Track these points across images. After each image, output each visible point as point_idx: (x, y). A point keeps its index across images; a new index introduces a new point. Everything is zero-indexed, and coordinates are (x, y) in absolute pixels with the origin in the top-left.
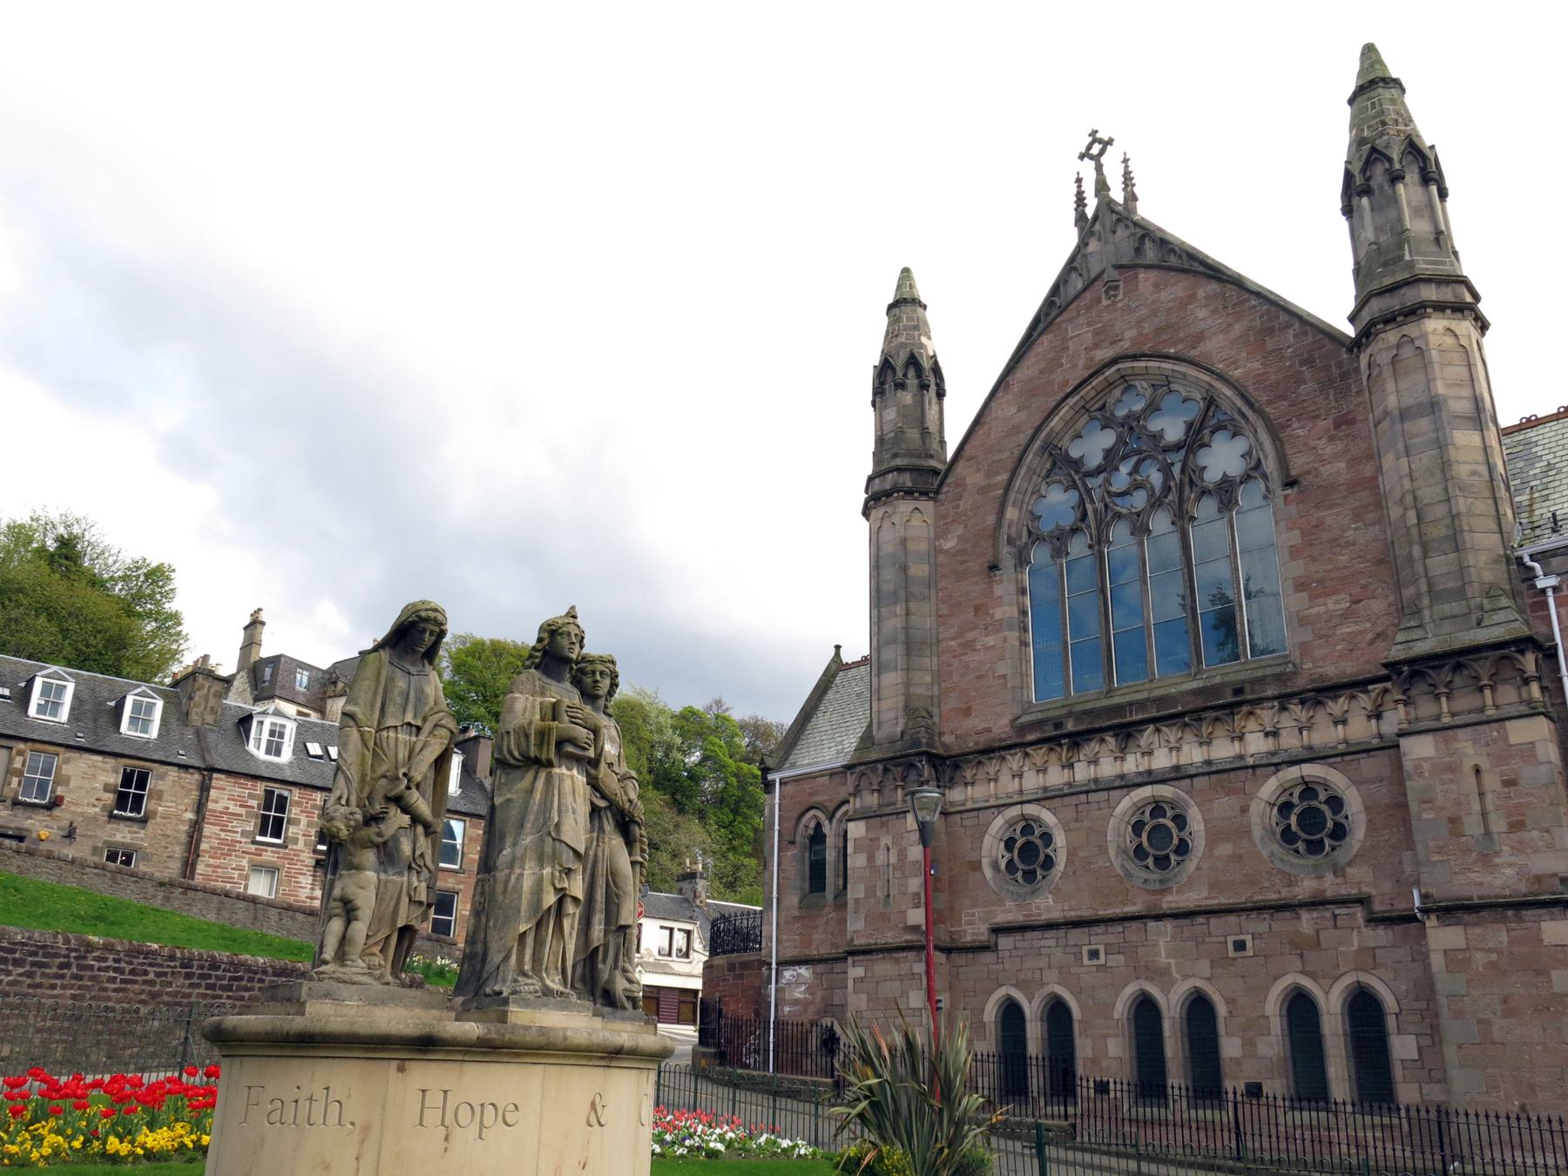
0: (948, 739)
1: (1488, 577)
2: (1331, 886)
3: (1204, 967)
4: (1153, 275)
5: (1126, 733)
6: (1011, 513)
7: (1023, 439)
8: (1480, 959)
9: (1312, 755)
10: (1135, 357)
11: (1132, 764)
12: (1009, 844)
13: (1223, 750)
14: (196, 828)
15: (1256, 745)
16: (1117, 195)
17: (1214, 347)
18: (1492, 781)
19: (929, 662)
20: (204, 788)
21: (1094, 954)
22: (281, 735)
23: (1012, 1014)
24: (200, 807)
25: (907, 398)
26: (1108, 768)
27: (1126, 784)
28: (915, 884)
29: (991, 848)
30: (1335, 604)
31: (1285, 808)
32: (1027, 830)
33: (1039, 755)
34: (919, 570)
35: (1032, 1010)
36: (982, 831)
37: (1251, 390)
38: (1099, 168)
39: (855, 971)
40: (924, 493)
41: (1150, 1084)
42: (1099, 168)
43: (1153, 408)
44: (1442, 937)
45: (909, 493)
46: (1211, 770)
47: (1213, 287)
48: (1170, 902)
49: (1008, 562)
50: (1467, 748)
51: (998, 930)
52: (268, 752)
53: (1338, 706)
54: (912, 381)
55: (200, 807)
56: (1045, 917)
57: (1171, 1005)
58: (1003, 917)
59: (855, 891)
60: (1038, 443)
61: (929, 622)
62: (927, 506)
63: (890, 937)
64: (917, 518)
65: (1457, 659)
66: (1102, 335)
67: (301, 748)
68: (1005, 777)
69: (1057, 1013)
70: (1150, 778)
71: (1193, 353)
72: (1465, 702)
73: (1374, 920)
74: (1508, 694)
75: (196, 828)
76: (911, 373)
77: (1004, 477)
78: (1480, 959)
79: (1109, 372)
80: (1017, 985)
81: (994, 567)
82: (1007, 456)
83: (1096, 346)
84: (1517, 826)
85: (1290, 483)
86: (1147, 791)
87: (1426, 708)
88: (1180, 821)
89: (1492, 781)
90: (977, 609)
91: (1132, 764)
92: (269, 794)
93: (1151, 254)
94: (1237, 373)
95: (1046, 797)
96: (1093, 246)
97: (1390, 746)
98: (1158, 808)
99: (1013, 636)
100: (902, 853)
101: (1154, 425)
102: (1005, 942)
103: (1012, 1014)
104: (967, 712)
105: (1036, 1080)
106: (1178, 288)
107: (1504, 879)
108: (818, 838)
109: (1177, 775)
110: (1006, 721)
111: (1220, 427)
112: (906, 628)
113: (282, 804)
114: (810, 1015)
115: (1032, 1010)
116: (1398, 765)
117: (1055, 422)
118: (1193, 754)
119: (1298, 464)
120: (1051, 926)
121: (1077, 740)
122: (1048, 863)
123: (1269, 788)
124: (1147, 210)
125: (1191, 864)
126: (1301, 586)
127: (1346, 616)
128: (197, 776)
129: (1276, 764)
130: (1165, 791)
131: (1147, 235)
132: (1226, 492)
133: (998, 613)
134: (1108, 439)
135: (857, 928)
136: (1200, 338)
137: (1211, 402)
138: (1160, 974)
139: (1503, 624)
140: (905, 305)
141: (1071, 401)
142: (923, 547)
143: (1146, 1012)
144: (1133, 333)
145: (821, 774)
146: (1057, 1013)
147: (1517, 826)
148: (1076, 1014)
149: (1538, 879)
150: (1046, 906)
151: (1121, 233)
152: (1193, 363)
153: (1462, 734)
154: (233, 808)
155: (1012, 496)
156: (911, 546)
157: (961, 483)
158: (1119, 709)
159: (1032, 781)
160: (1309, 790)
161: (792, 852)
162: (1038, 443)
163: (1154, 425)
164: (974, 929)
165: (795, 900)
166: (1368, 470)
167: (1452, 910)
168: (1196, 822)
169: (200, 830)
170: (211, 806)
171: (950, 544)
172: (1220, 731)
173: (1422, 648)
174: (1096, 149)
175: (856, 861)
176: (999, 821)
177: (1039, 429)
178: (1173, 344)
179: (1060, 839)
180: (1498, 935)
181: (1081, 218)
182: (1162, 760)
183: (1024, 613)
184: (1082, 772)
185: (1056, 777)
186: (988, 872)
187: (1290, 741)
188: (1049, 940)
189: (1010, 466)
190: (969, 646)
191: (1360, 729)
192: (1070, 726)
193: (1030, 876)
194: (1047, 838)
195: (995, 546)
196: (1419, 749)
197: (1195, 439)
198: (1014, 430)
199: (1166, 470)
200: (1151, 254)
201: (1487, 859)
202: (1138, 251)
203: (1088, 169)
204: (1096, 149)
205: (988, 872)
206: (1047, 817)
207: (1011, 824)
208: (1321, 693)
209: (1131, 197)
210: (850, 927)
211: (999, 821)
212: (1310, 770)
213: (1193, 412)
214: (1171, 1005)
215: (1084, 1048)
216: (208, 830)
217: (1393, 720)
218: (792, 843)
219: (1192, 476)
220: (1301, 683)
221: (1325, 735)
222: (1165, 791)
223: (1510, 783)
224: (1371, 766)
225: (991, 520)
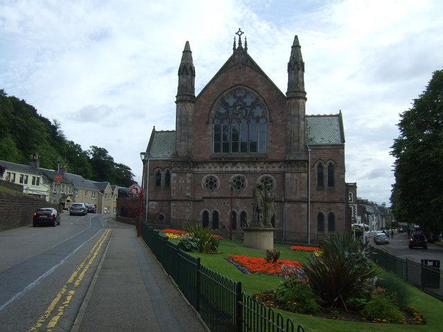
0: (194, 158)
3: (245, 207)
4: (249, 69)
5: (235, 163)
6: (213, 112)
11: (234, 169)
12: (207, 181)
13: (252, 169)
15: (259, 169)
16: (244, 47)
17: (260, 89)
18: (298, 182)
21: (224, 204)
23: (206, 214)
26: (229, 169)
27: (233, 173)
28: (188, 188)
29: (203, 181)
30: (276, 146)
32: (211, 179)
33: (216, 164)
35: (210, 213)
36: (201, 178)
37: (266, 101)
38: (240, 38)
39: (173, 204)
41: (233, 226)
42: (240, 38)
43: (245, 97)
44: (287, 205)
46: (250, 172)
47: (259, 76)
48: (240, 195)
50: (295, 176)
51: (204, 198)
53: (274, 165)
56: (214, 196)
57: (238, 213)
58: (205, 195)
59: (173, 188)
62: (193, 105)
63: (182, 198)
64: (190, 107)
65: (296, 162)
68: (207, 167)
69: (216, 214)
70: (238, 172)
72: (296, 168)
73: (275, 202)
74: (303, 168)
77: (212, 103)
80: (208, 208)
83: (236, 80)
85: (271, 122)
86: (237, 175)
87: (290, 168)
88: (243, 181)
89: (298, 182)
90: (203, 131)
91: (234, 169)
93: (249, 63)
95: (217, 173)
96: (236, 56)
97: (283, 173)
98: (239, 178)
100: (185, 181)
101: (245, 100)
102: (206, 200)
103: (206, 214)
104: (200, 153)
105: (210, 225)
106: (253, 74)
107: (298, 197)
108: (159, 174)
109: (243, 172)
110: (208, 156)
111: (258, 105)
114: (156, 212)
115: (210, 213)
116: (284, 176)
118: (246, 169)
119: (273, 118)
120: (217, 198)
121: (224, 163)
122: (215, 186)
124: (249, 52)
125: (245, 189)
126: (271, 142)
130: (241, 175)
131: (249, 59)
132: (258, 119)
133: (208, 133)
134: (235, 100)
135: (174, 195)
136: (257, 86)
137: (257, 99)
138: (238, 208)
139: (303, 157)
140: (187, 52)
143: (234, 213)
145: (160, 160)
146: (216, 214)
147: (301, 189)
148: (220, 214)
149: (303, 198)
150: (215, 194)
151: (243, 56)
152: (255, 91)
155: (213, 108)
158: (233, 158)
159: (213, 169)
161: (152, 176)
163: (245, 100)
164: (199, 197)
165: (153, 187)
166: (285, 123)
167: (289, 202)
168: (246, 182)
171: (198, 115)
173: (291, 158)
174: (240, 33)
175: (173, 182)
176: (206, 177)
179: (219, 181)
180: (295, 206)
181: (234, 48)
182: (240, 169)
184: (224, 169)
185: (218, 169)
186: (203, 187)
187: (265, 169)
188: (215, 200)
191: (277, 169)
192: (223, 160)
193: (211, 188)
194: (215, 181)
195: (208, 119)
196: (288, 175)
197: (253, 106)
199: (246, 111)
200: (249, 63)
201: (296, 194)
202: (247, 61)
203: (237, 37)
204: (240, 33)
205: (203, 187)
206: (216, 177)
207: (208, 177)
208: (272, 162)
209: (246, 48)
210: (172, 195)
211: (206, 177)
212: (269, 175)
213: (253, 100)
214: (238, 213)
215: (221, 220)
217: (282, 169)
218: (152, 175)
219: (252, 114)
221: (271, 169)
222: (241, 175)
224: (278, 176)
225: (208, 112)
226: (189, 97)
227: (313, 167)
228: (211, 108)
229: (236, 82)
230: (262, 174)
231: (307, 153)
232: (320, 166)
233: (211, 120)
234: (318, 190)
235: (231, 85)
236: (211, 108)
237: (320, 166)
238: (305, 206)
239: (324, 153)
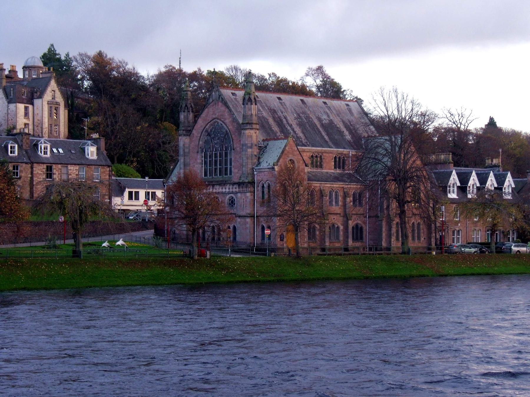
1: (249, 172)
2: (232, 212)
6: (201, 143)
7: (202, 128)
8: (241, 223)
9: (232, 193)
10: (218, 119)
13: (224, 190)
14: (32, 178)
19: (188, 168)
20: (32, 168)
22: (47, 148)
24: (32, 173)
25: (186, 114)
31: (230, 200)
34: (187, 150)
40: (187, 135)
45: (185, 135)
49: (200, 152)
52: (44, 154)
54: (186, 110)
55: (32, 173)
60: (204, 131)
61: (188, 160)
62: (188, 137)
66: (214, 113)
67: (52, 151)
71: (225, 122)
72: (245, 189)
75: (32, 178)
76: (186, 108)
77: (200, 135)
78: (241, 223)
79: (214, 120)
81: (198, 152)
82: (200, 131)
84: (246, 207)
85: (234, 150)
87: (241, 189)
92: (47, 167)
94: (229, 128)
99: (200, 166)
112: (184, 162)
113: (51, 167)
117: (207, 127)
118: (220, 190)
123: (228, 197)
127: (237, 173)
128: (30, 165)
129: (229, 193)
136: (225, 119)
141: (210, 124)
142: (188, 146)
144: (217, 114)
151: (217, 93)
153: (243, 194)
154: (40, 172)
156: (186, 146)
157: (193, 134)
160: (232, 198)
162: (204, 131)
169: (33, 179)
170: (34, 172)
172: (224, 187)
177: (205, 127)
178: (223, 118)
180: (243, 220)
183: (203, 161)
187: (231, 190)
189: (200, 133)
190: (194, 166)
198: (201, 126)
201: (243, 210)
202: (219, 98)
212: (232, 195)
216: (35, 179)
220: (232, 182)
223: (246, 201)
226: (184, 132)
227: (258, 187)
228: (200, 139)
229: (214, 116)
230: (229, 194)
231: (253, 175)
232: (263, 187)
233: (199, 150)
234: (261, 206)
235: (210, 119)
236: (200, 139)
237: (263, 187)
238: (248, 220)
239: (264, 175)
